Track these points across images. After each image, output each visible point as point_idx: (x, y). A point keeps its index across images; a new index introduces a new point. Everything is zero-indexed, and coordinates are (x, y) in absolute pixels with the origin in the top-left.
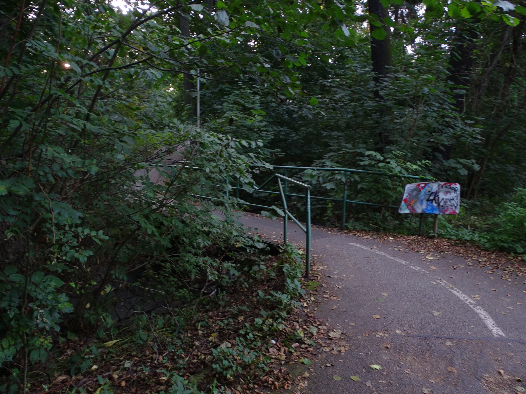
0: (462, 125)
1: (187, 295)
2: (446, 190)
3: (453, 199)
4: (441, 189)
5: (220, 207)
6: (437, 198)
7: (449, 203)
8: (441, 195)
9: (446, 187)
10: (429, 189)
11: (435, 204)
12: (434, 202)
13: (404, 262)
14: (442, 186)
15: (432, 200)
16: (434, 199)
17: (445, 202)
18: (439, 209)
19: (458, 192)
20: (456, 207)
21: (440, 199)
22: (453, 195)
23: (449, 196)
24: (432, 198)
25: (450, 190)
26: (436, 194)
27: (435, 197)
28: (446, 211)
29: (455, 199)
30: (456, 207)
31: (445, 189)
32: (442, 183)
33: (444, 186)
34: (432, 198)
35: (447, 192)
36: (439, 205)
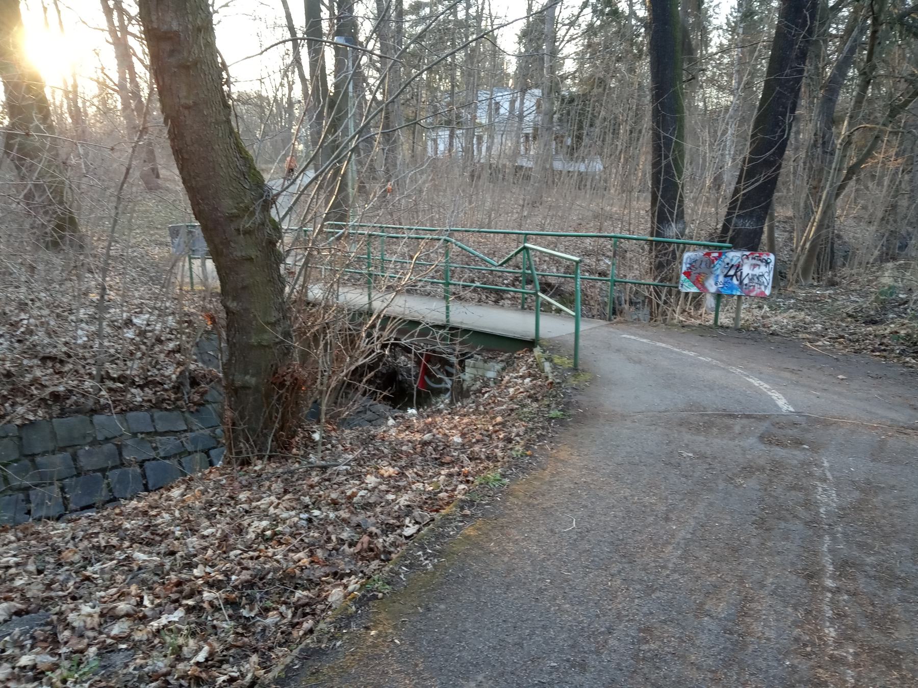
0: (307, 645)
1: (248, 537)
2: (754, 262)
3: (763, 275)
4: (746, 261)
5: (57, 515)
6: (739, 273)
7: (756, 281)
8: (746, 270)
9: (754, 258)
10: (727, 260)
11: (735, 281)
12: (734, 278)
13: (692, 354)
14: (747, 257)
15: (732, 276)
16: (735, 274)
17: (751, 280)
18: (741, 288)
19: (772, 265)
20: (766, 287)
21: (744, 275)
22: (763, 269)
23: (757, 271)
24: (732, 272)
25: (759, 262)
26: (738, 267)
27: (736, 272)
28: (751, 291)
29: (766, 275)
30: (766, 287)
31: (751, 261)
32: (748, 253)
33: (750, 257)
34: (732, 272)
35: (755, 266)
36: (741, 282)
